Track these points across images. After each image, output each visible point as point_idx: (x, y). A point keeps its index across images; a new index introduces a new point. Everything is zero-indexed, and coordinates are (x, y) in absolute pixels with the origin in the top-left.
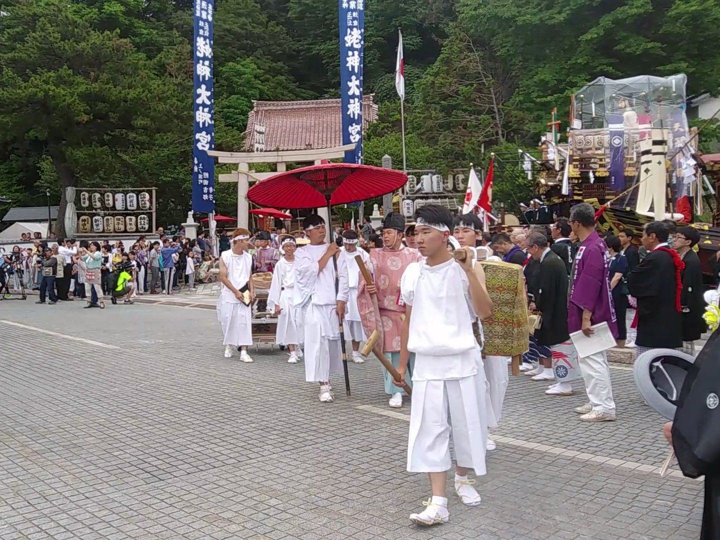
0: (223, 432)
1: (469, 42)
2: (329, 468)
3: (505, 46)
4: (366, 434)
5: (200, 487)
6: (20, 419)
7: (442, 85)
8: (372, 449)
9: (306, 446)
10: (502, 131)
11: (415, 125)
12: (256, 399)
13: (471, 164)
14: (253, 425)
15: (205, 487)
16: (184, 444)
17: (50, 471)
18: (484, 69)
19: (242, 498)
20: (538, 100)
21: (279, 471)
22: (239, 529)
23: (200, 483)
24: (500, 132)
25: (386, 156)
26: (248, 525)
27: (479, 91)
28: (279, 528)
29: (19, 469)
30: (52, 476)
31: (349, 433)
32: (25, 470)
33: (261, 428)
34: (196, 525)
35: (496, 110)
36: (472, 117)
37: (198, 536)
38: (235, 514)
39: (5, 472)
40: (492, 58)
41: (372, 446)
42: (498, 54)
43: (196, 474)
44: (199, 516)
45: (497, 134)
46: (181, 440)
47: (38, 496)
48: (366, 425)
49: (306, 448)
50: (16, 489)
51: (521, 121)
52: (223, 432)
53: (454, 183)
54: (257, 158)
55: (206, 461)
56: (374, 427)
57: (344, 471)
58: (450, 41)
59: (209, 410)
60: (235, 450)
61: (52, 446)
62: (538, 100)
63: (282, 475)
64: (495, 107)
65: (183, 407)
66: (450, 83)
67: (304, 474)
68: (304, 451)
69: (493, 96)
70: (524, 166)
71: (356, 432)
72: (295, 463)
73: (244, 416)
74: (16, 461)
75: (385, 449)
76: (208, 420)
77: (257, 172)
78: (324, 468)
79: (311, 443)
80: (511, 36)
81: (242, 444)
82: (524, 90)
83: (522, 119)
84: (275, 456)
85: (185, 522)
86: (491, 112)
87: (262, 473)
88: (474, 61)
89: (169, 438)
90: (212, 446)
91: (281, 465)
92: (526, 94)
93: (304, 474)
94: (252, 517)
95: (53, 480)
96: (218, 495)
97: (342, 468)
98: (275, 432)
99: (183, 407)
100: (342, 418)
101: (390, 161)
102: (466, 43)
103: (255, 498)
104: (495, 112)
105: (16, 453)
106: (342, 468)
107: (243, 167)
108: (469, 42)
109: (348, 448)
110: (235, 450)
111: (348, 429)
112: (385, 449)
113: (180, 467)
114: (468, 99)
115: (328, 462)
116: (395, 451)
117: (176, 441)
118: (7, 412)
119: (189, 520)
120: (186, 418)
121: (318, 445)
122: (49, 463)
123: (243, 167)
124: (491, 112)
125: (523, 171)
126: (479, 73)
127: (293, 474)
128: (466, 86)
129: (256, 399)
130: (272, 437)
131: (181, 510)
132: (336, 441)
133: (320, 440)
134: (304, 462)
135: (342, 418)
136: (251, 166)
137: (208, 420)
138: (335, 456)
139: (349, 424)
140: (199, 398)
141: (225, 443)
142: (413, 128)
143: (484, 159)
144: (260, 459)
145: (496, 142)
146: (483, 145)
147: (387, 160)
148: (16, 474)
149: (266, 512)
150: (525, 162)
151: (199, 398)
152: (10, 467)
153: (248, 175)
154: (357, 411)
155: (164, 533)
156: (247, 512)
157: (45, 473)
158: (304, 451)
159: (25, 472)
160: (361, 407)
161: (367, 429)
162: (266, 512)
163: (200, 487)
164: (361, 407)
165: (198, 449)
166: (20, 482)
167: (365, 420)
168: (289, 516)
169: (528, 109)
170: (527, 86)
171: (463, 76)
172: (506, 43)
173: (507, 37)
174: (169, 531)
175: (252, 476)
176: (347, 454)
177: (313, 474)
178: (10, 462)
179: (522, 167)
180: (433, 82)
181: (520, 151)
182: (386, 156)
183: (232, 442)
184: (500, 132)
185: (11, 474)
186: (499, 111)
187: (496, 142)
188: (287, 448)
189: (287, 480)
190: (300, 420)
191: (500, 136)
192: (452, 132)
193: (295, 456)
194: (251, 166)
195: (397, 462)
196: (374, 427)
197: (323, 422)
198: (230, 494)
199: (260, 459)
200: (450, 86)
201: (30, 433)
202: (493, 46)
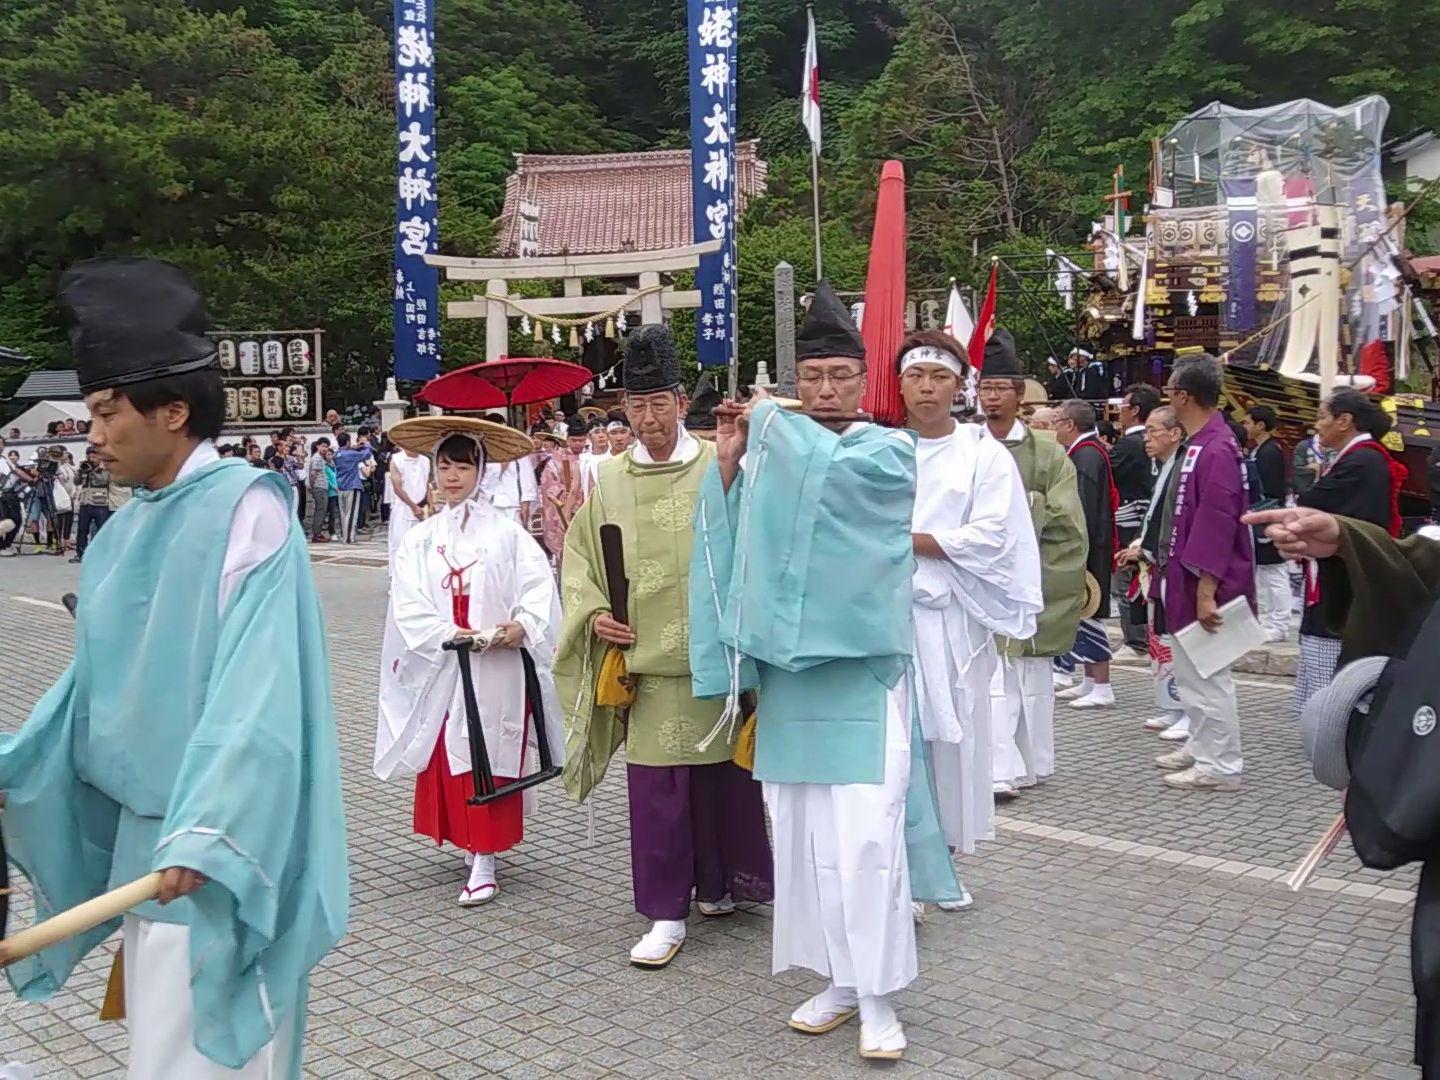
1: (949, 32)
3: (1021, 42)
7: (897, 120)
10: (1015, 213)
11: (841, 202)
13: (953, 279)
15: (421, 922)
16: (380, 838)
18: (979, 87)
19: (497, 942)
20: (1088, 151)
22: (489, 1004)
24: (1010, 216)
25: (783, 265)
26: (508, 996)
27: (970, 132)
28: (568, 1001)
34: (404, 998)
35: (1002, 171)
36: (955, 185)
37: (407, 1019)
38: (481, 976)
40: (997, 65)
42: (1008, 56)
44: (411, 979)
45: (1004, 216)
46: (373, 831)
51: (1054, 192)
53: (918, 318)
54: (526, 269)
58: (911, 32)
62: (1088, 151)
64: (1001, 163)
66: (913, 117)
67: (619, 896)
69: (997, 142)
70: (1057, 283)
80: (1034, 19)
82: (1060, 131)
83: (1057, 188)
84: (562, 860)
85: (381, 991)
86: (991, 173)
88: (957, 72)
92: (1063, 138)
93: (619, 896)
94: (514, 979)
96: (448, 937)
101: (791, 275)
102: (942, 36)
103: (521, 943)
104: (999, 175)
107: (497, 288)
108: (949, 32)
113: (372, 883)
114: (949, 150)
119: (390, 987)
123: (497, 288)
124: (991, 173)
125: (1056, 293)
126: (969, 96)
127: (595, 896)
128: (946, 122)
131: (374, 967)
136: (512, 286)
142: (838, 208)
143: (977, 270)
145: (1003, 236)
146: (975, 242)
147: (785, 271)
149: (543, 969)
150: (1060, 275)
153: (505, 304)
155: (340, 1013)
156: (506, 971)
162: (543, 969)
168: (588, 978)
169: (1067, 169)
170: (1064, 122)
171: (937, 100)
172: (1023, 34)
173: (1024, 22)
174: (350, 1009)
179: (1053, 285)
180: (877, 116)
181: (1050, 252)
182: (783, 265)
184: (1010, 216)
186: (1008, 173)
187: (1003, 236)
189: (585, 907)
191: (1011, 223)
192: (915, 216)
194: (512, 286)
198: (472, 934)
200: (912, 121)
202: (995, 41)
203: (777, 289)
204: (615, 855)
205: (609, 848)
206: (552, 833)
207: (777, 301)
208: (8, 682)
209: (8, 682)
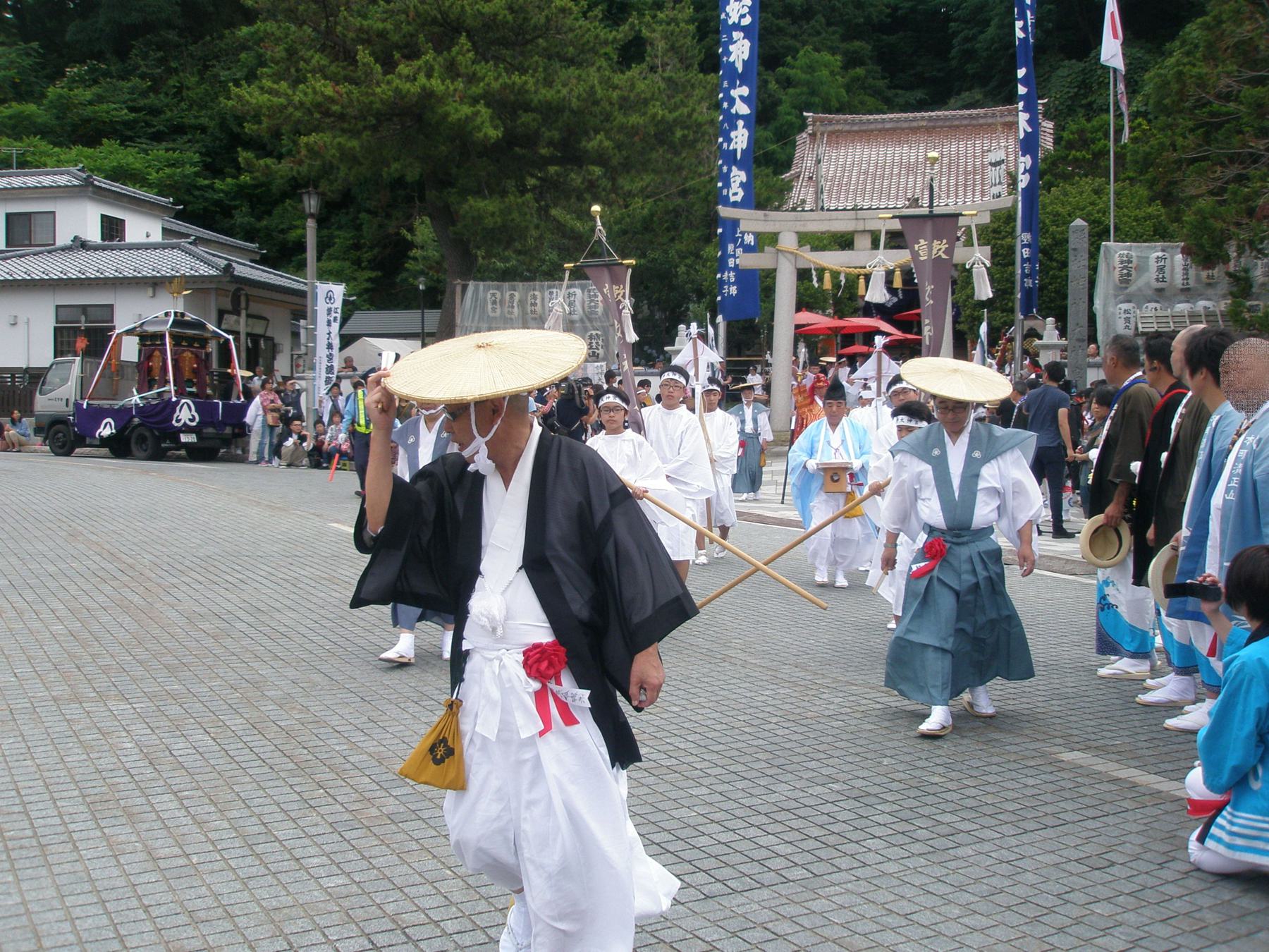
0: (773, 798)
2: (1022, 909)
4: (1091, 824)
5: (734, 934)
6: (358, 737)
8: (1113, 864)
9: (960, 845)
12: (835, 724)
14: (835, 786)
16: (692, 822)
17: (415, 865)
21: (907, 907)
23: (733, 925)
25: (1079, 222)
29: (352, 855)
30: (418, 879)
31: (1049, 821)
32: (364, 857)
33: (855, 793)
39: (324, 860)
41: (1112, 856)
43: (725, 901)
46: (683, 812)
47: (391, 926)
48: (1087, 801)
49: (960, 852)
50: (346, 903)
52: (773, 798)
55: (743, 868)
56: (1106, 808)
57: (1059, 921)
59: (740, 745)
60: (804, 845)
61: (419, 806)
63: (914, 917)
65: (683, 732)
67: (965, 920)
68: (957, 858)
71: (1068, 817)
72: (941, 889)
73: (813, 764)
74: (347, 835)
75: (1142, 866)
76: (739, 768)
77: (814, 249)
78: (1008, 908)
79: (969, 839)
81: (816, 832)
84: (891, 868)
87: (871, 911)
89: (660, 806)
90: (752, 832)
91: (908, 892)
93: (965, 920)
95: (422, 890)
97: (1051, 910)
98: (886, 808)
99: (683, 732)
100: (1031, 782)
101: (1086, 231)
105: (346, 816)
106: (1051, 910)
107: (788, 241)
109: (1057, 859)
110: (804, 845)
111: (1049, 809)
112: (1142, 866)
115: (1016, 890)
116: (1166, 874)
117: (674, 813)
118: (335, 721)
120: (691, 759)
121: (986, 847)
122: (414, 846)
123: (788, 241)
129: (835, 724)
130: (881, 819)
132: (1025, 838)
133: (988, 834)
134: (960, 888)
135: (1031, 782)
137: (739, 768)
138: (1030, 878)
139: (1048, 798)
140: (715, 715)
141: (779, 828)
144: (859, 873)
147: (1081, 229)
148: (347, 868)
151: (715, 715)
152: (336, 847)
154: (1059, 766)
157: (405, 869)
158: (957, 858)
159: (365, 864)
160: (1067, 756)
161: (1091, 813)
163: (734, 934)
164: (1067, 756)
165: (724, 837)
166: (354, 889)
167: (1082, 790)
175: (849, 916)
176: (1055, 874)
177: (985, 922)
178: (336, 837)
182: (1079, 222)
183: (795, 824)
185: (338, 865)
188: (917, 848)
190: (936, 779)
193: (938, 871)
195: (1177, 904)
196: (1106, 808)
197: (988, 788)
199: (859, 873)
201: (377, 770)
203: (1071, 245)
204: (953, 865)
205: (946, 856)
206: (878, 831)
207: (1071, 258)
208: (323, 612)
209: (323, 612)
